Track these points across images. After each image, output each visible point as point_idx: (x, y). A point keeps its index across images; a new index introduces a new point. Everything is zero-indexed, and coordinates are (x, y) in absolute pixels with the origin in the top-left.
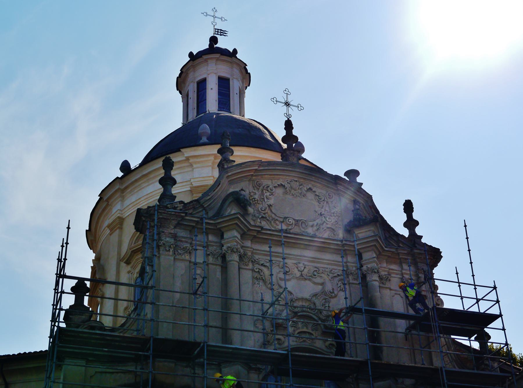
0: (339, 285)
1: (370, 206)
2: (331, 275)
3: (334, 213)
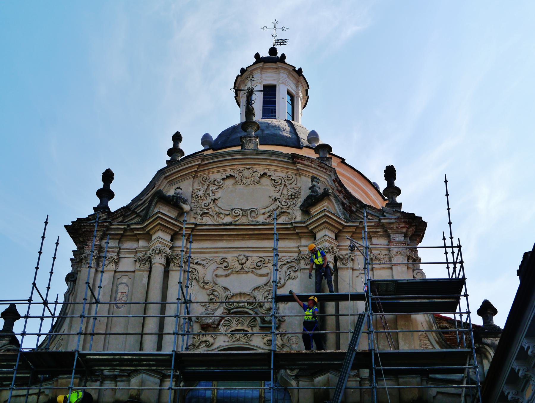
1: (333, 180)
3: (292, 195)
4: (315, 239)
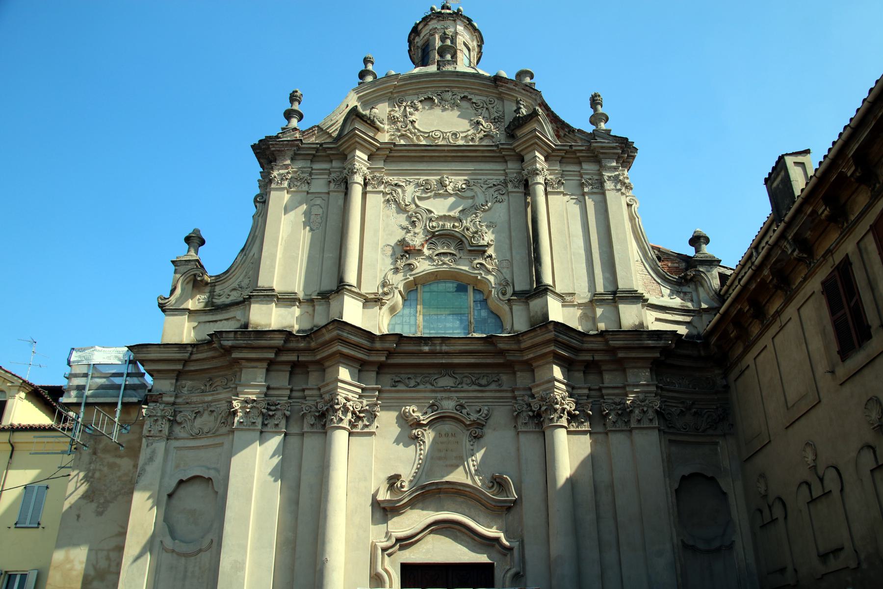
0: (495, 196)
2: (486, 186)
4: (523, 161)
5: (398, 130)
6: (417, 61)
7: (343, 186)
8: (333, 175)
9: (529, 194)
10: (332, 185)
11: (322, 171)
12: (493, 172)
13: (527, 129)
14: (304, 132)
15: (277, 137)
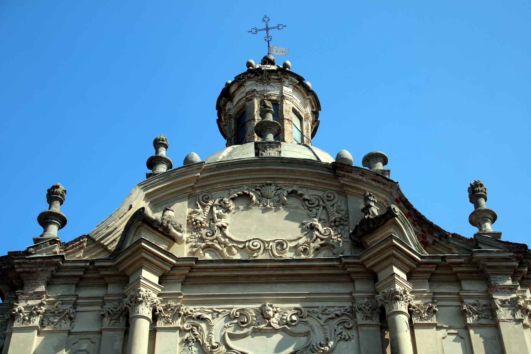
2: (325, 317)
3: (335, 221)
5: (202, 239)
6: (229, 136)
7: (122, 321)
8: (108, 306)
9: (387, 328)
10: (106, 320)
11: (92, 301)
12: (334, 296)
13: (380, 236)
14: (67, 245)
15: (27, 253)
